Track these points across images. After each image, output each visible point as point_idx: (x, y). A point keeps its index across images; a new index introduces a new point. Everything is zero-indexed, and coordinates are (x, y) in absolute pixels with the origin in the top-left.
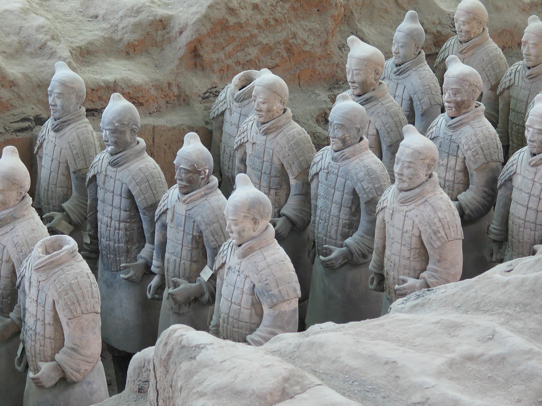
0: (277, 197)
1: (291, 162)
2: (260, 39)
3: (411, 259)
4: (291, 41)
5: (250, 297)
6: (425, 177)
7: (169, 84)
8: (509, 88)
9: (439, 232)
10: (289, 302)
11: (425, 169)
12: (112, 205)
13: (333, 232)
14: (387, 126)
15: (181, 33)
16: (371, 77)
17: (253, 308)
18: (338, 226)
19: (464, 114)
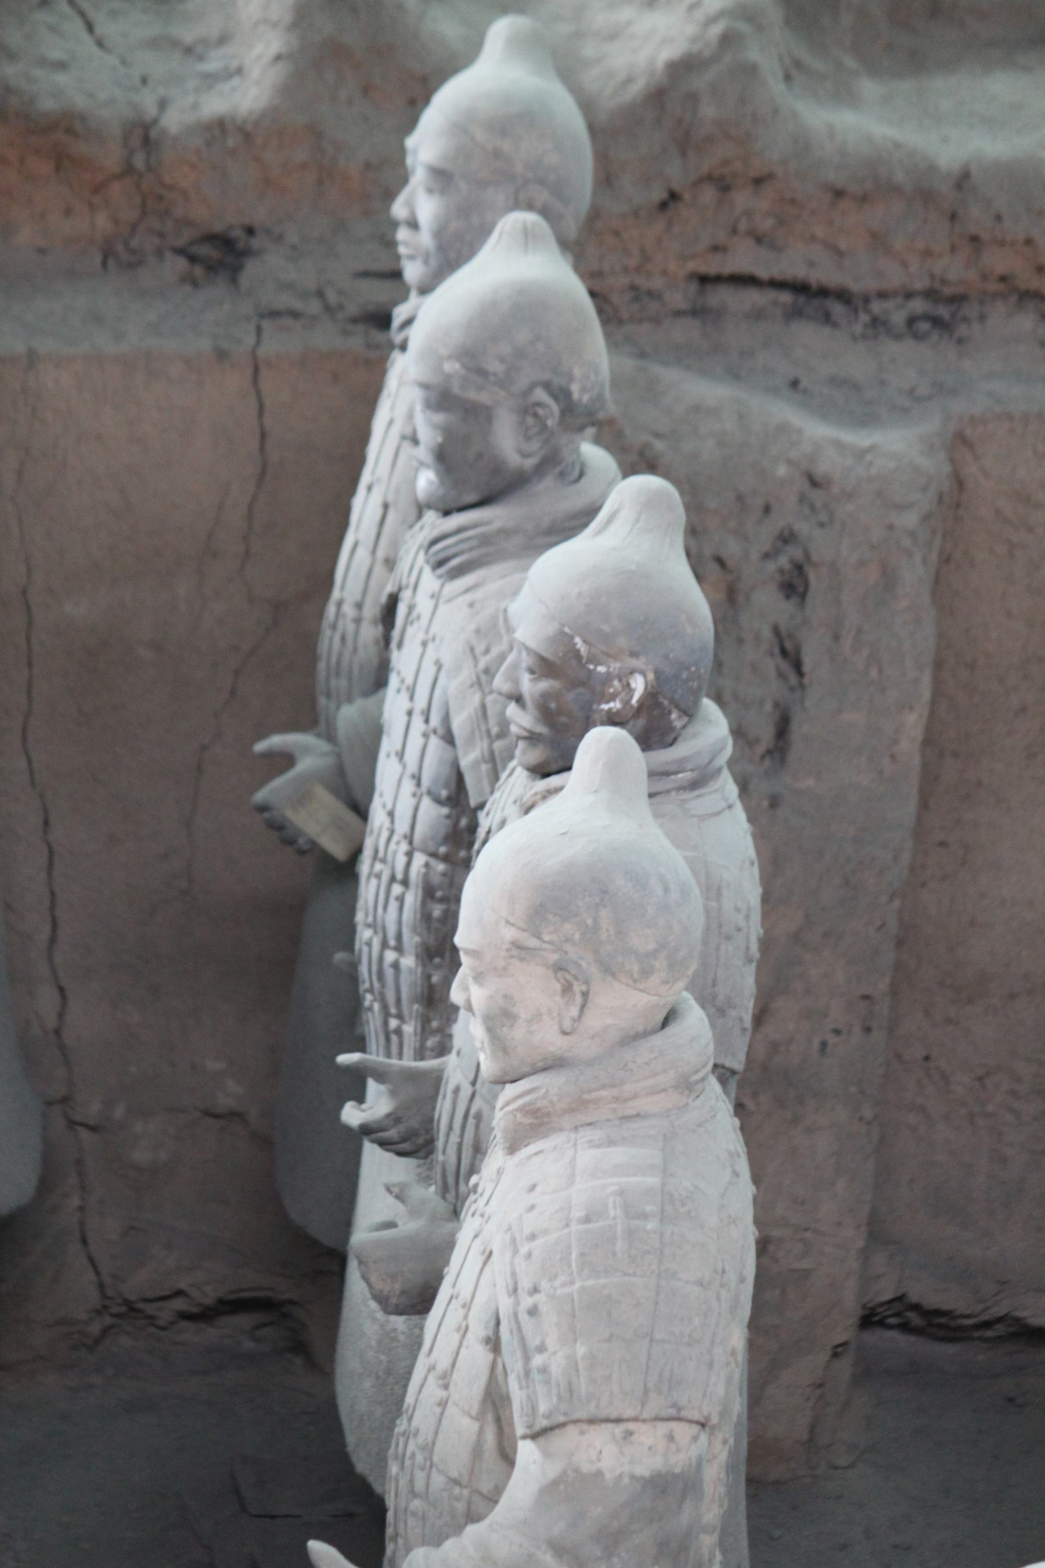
10: (619, 1429)
17: (490, 1417)
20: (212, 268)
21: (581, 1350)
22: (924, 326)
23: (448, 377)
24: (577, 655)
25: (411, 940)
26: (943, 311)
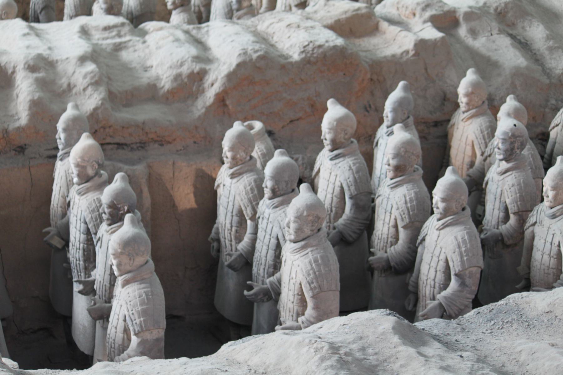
0: (238, 234)
1: (246, 206)
2: (284, 95)
3: (295, 303)
4: (315, 99)
5: (123, 323)
6: (310, 232)
7: (196, 127)
8: (490, 156)
9: (313, 283)
10: (150, 332)
11: (309, 225)
12: (76, 228)
13: (262, 270)
14: (348, 181)
15: (212, 85)
16: (340, 136)
17: (125, 333)
18: (265, 265)
19: (400, 176)
20: (19, 152)
21: (142, 319)
22: (140, 148)
23: (78, 162)
24: (115, 204)
25: (81, 259)
26: (143, 145)
